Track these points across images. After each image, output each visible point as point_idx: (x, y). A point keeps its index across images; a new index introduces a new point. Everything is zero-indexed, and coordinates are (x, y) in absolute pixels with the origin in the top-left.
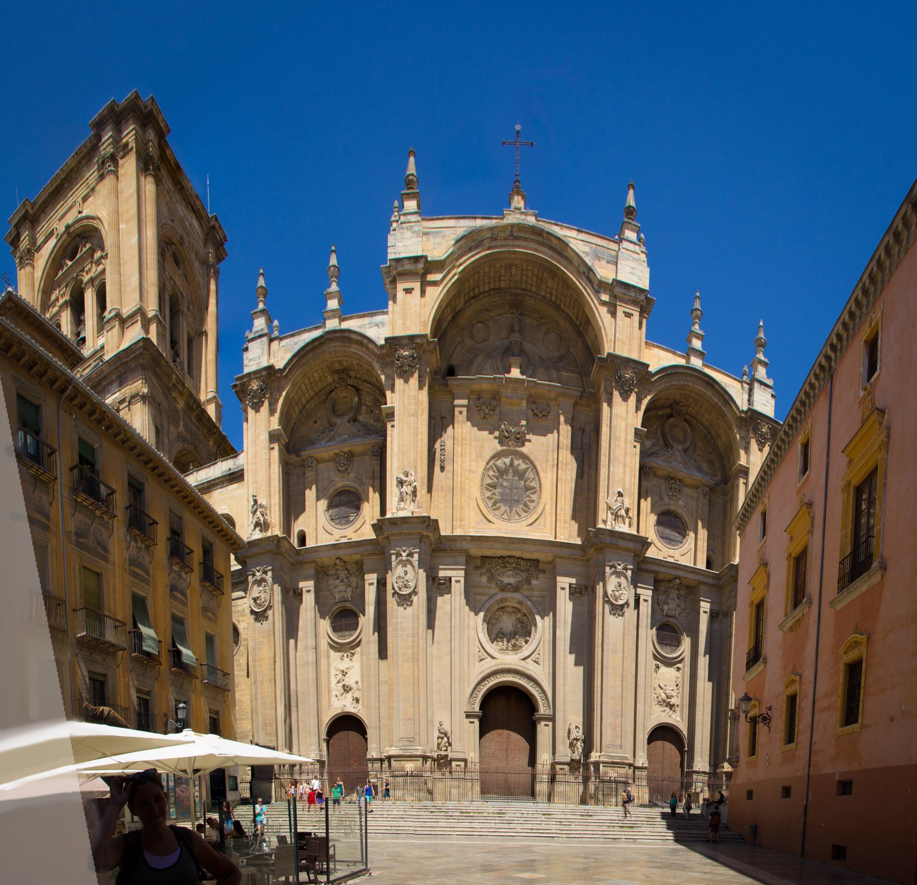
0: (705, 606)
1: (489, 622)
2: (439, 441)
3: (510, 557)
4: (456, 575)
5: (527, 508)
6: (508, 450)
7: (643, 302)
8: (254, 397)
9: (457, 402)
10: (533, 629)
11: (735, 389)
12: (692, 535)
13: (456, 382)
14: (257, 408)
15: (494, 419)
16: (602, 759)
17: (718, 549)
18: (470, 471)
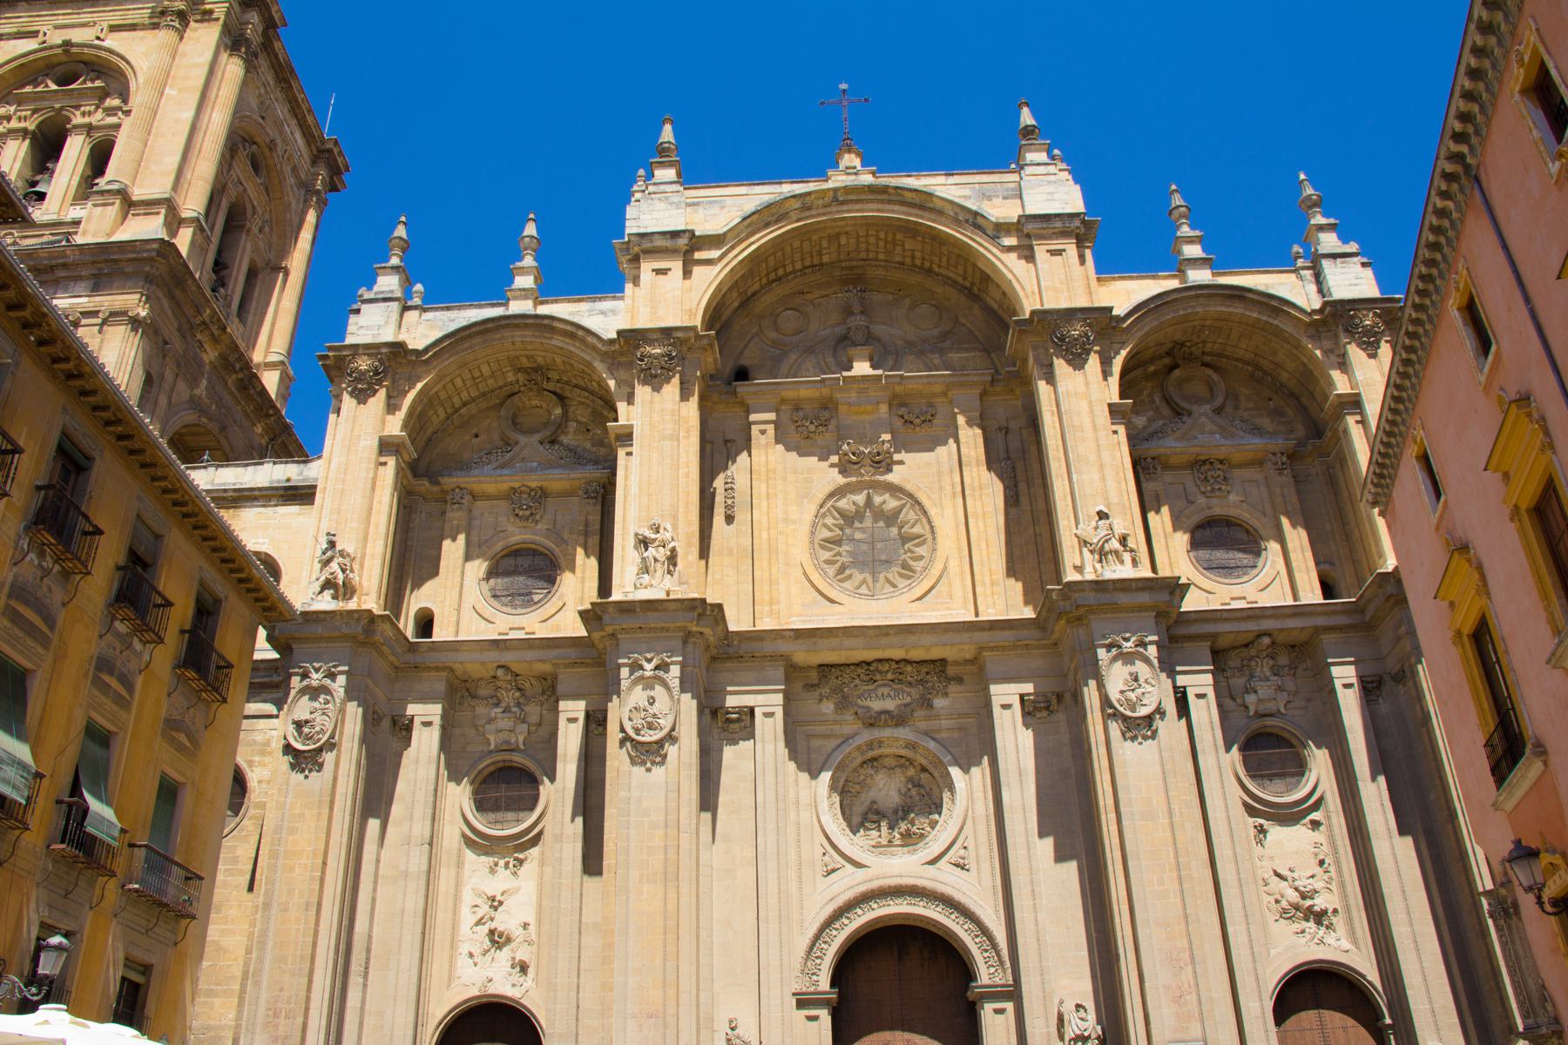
0: (1344, 674)
1: (844, 790)
2: (722, 476)
3: (880, 661)
4: (767, 704)
5: (907, 571)
7: (1079, 230)
8: (358, 380)
9: (753, 417)
10: (946, 795)
12: (1273, 546)
13: (752, 389)
14: (362, 396)
15: (827, 437)
17: (1338, 552)
18: (786, 520)
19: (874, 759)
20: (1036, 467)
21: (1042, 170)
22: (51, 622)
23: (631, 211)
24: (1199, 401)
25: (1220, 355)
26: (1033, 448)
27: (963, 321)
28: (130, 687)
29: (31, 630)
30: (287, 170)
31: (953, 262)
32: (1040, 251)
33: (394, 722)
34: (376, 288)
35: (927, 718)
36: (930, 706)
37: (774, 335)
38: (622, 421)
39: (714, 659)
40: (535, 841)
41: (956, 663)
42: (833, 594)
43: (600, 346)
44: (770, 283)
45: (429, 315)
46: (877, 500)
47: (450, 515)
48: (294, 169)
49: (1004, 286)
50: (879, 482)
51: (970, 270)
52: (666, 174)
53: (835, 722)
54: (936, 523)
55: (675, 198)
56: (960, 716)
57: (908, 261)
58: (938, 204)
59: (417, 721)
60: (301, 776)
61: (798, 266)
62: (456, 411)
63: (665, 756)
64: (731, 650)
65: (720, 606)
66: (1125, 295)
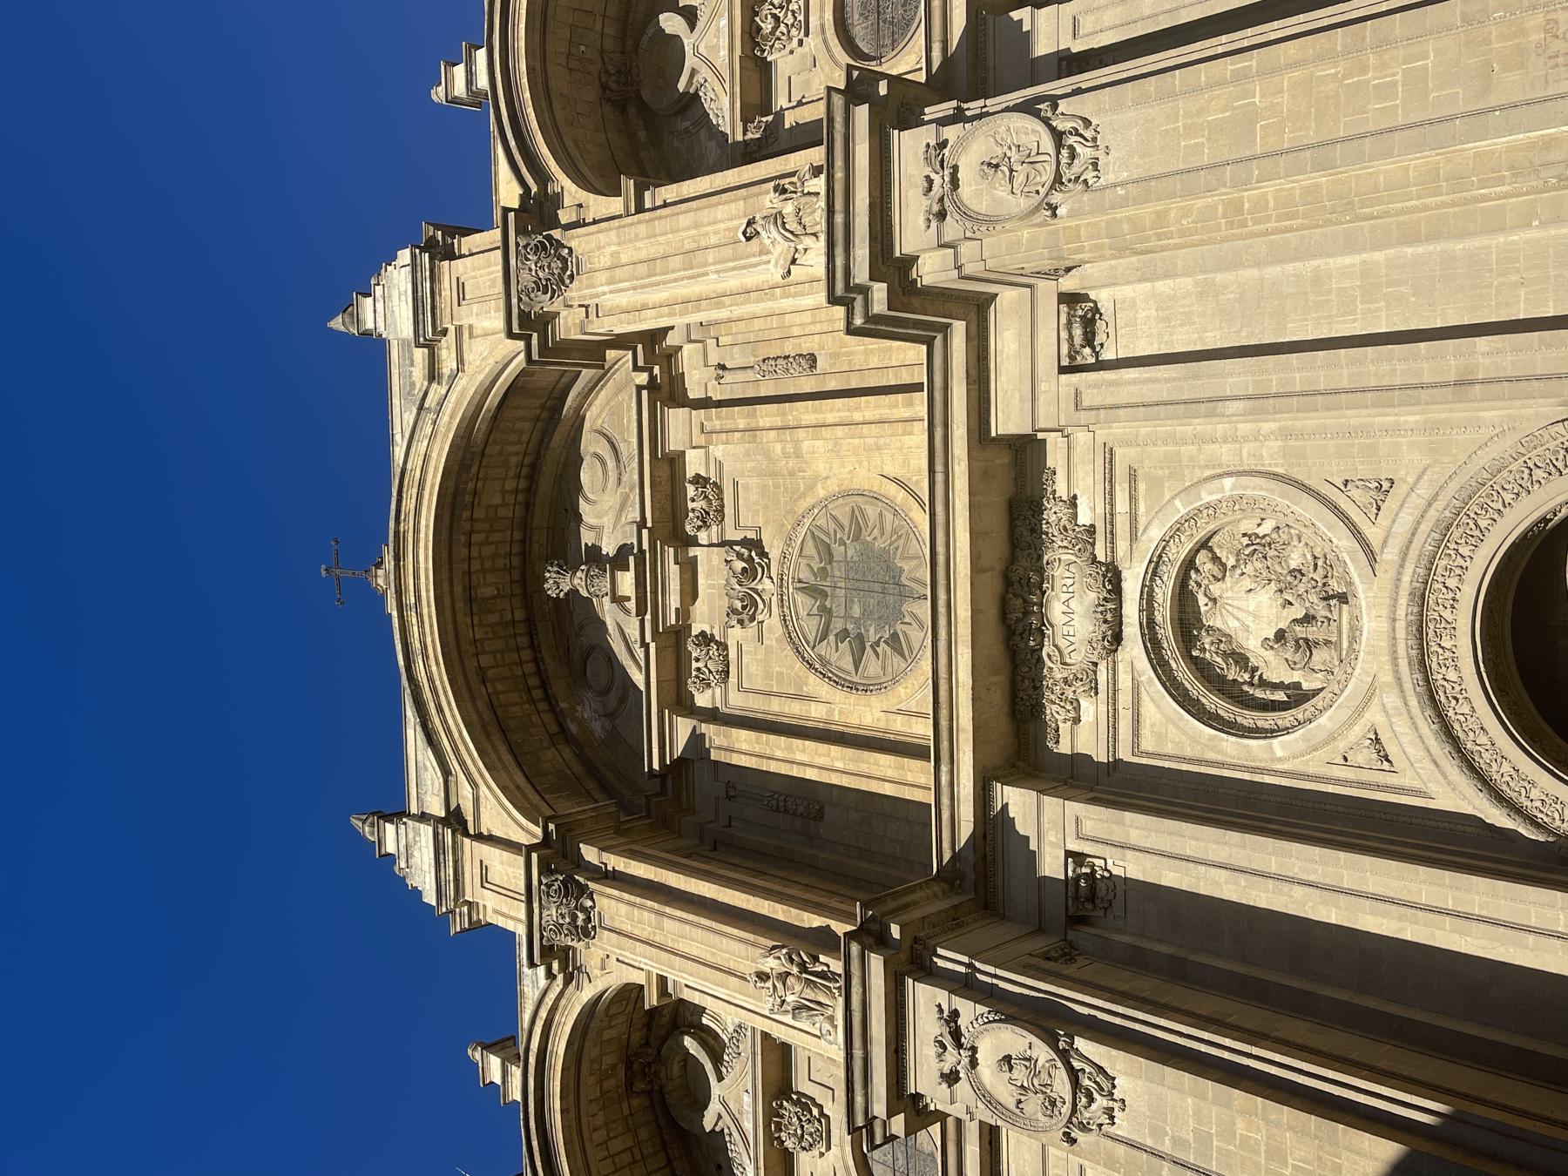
20: (757, 324)
21: (380, 306)
26: (735, 327)
31: (514, 437)
32: (467, 316)
36: (1091, 530)
37: (613, 699)
39: (986, 907)
43: (558, 990)
44: (548, 698)
51: (521, 413)
52: (391, 837)
54: (833, 486)
55: (411, 836)
56: (1110, 480)
57: (521, 497)
58: (415, 462)
61: (526, 655)
63: (1101, 1070)
64: (971, 876)
65: (865, 906)
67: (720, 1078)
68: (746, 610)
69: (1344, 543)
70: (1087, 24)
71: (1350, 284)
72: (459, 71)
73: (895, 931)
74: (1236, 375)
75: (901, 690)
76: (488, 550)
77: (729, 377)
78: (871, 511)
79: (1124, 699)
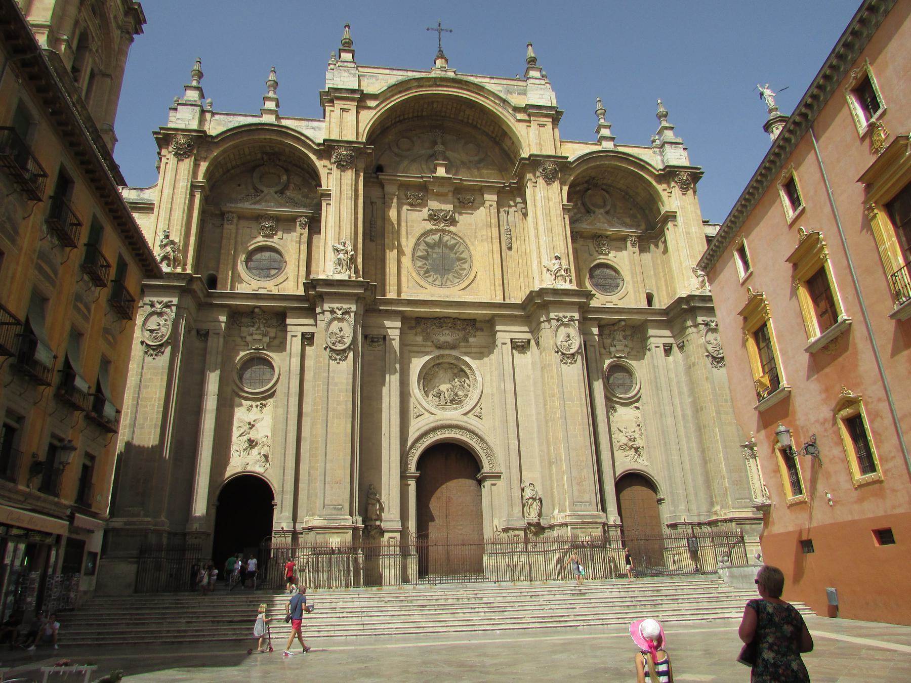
6: (436, 229)
11: (655, 160)
16: (568, 520)
19: (439, 364)
21: (537, 82)
22: (55, 272)
23: (328, 75)
24: (600, 207)
25: (610, 186)
27: (489, 154)
28: (89, 310)
29: (48, 278)
30: (112, 16)
32: (534, 125)
33: (198, 332)
34: (185, 98)
35: (466, 347)
36: (467, 341)
37: (396, 150)
38: (324, 187)
40: (271, 396)
41: (481, 321)
42: (422, 283)
45: (217, 117)
46: (446, 238)
47: (226, 226)
48: (115, 17)
49: (515, 140)
50: (445, 230)
53: (422, 346)
54: (473, 253)
57: (465, 120)
59: (210, 332)
60: (150, 359)
61: (411, 115)
62: (228, 171)
63: (347, 357)
66: (573, 151)
67: (276, 193)
68: (433, 217)
69: (468, 408)
70: (592, 349)
71: (530, 412)
72: (605, 132)
73: (368, 293)
74: (510, 386)
75: (414, 274)
76: (449, 107)
77: (505, 215)
78: (466, 266)
79: (423, 349)
